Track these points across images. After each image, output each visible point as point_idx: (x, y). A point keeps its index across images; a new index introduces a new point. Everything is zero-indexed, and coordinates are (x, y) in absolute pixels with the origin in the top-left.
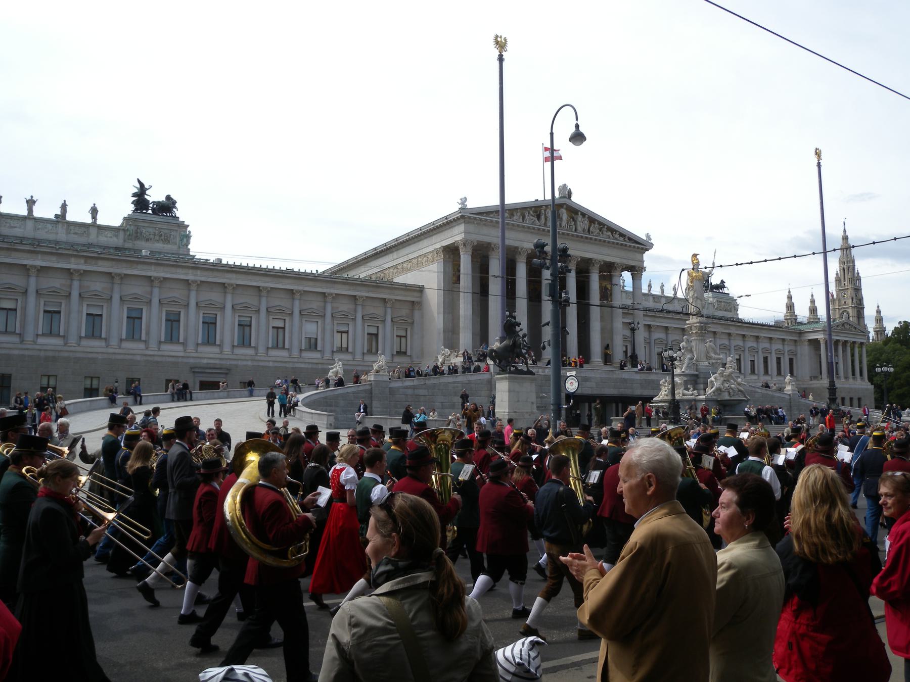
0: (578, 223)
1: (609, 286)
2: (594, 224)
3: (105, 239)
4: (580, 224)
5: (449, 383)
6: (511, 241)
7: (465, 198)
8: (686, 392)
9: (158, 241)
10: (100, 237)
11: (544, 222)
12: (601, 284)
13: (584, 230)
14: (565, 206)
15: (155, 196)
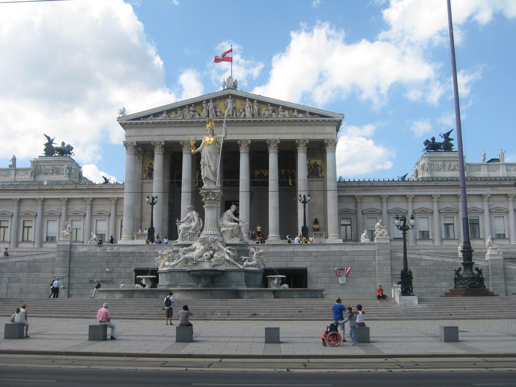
0: (246, 108)
1: (319, 162)
2: (268, 107)
3: (19, 177)
4: (247, 110)
5: (16, 262)
6: (173, 136)
7: (124, 108)
8: (167, 263)
9: (52, 174)
10: (17, 176)
11: (206, 114)
12: (309, 162)
13: (253, 116)
14: (230, 97)
15: (57, 144)
